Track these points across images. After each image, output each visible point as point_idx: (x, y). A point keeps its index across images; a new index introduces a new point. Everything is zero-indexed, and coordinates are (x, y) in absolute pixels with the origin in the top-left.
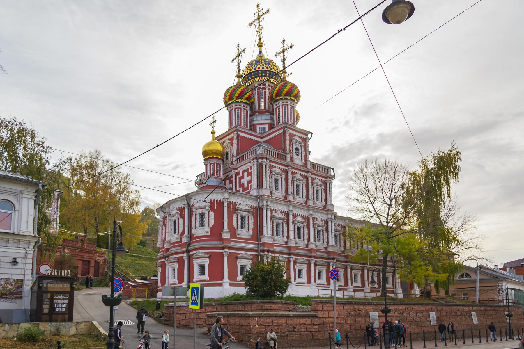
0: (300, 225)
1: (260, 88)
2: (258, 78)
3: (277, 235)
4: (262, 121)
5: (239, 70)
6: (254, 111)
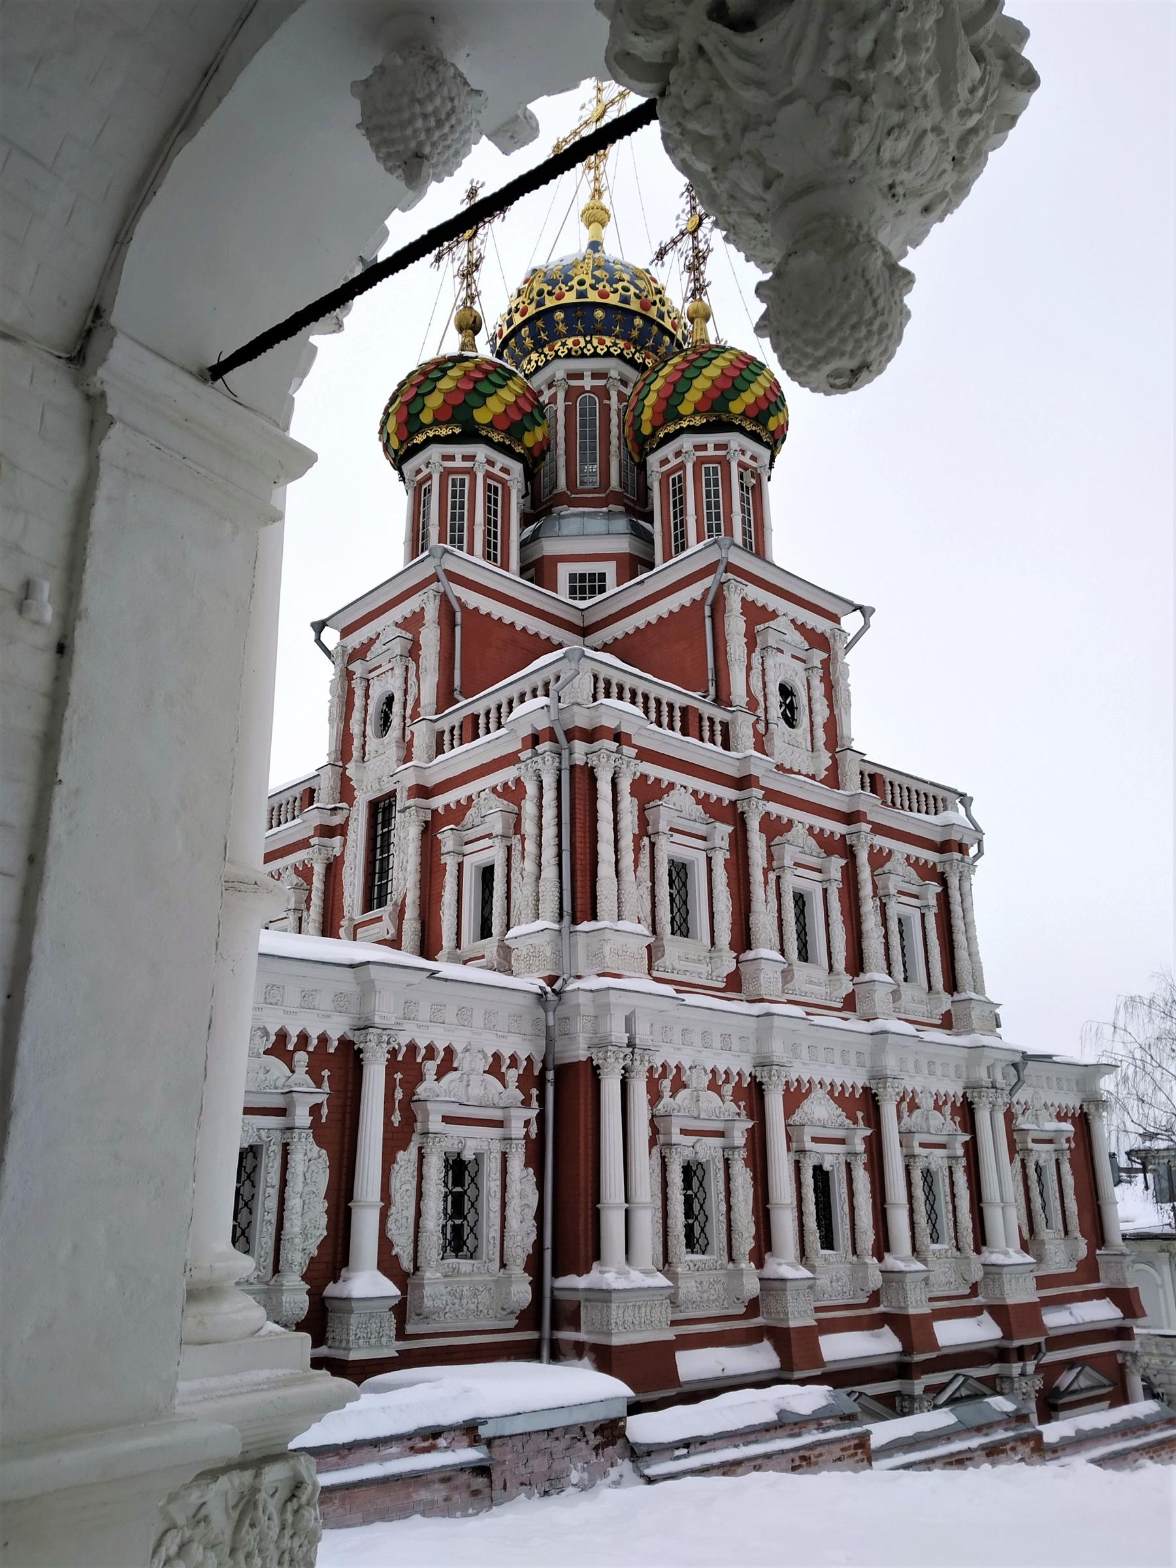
0: (831, 1157)
1: (582, 390)
2: (570, 342)
3: (691, 1244)
4: (587, 538)
5: (471, 298)
6: (544, 491)
